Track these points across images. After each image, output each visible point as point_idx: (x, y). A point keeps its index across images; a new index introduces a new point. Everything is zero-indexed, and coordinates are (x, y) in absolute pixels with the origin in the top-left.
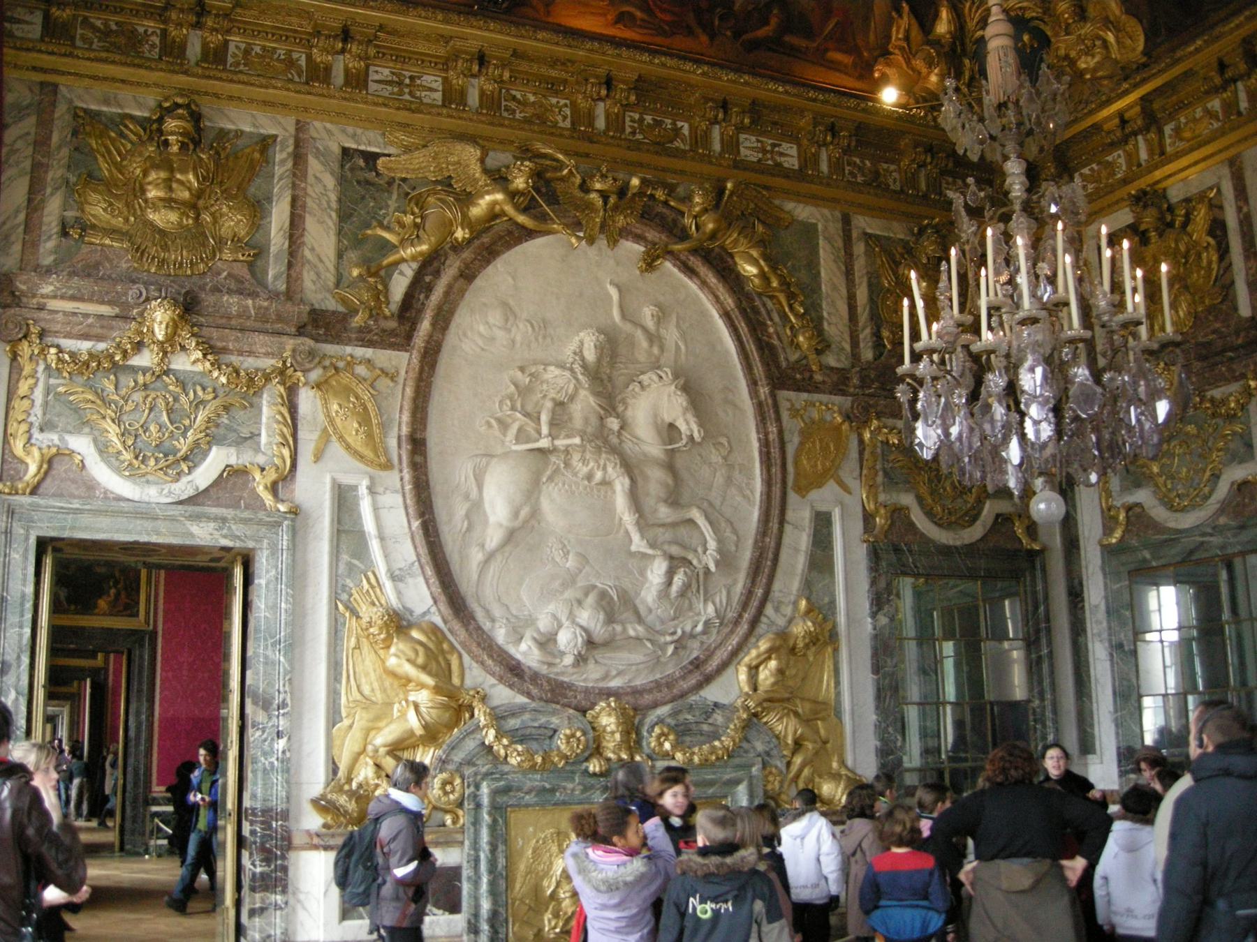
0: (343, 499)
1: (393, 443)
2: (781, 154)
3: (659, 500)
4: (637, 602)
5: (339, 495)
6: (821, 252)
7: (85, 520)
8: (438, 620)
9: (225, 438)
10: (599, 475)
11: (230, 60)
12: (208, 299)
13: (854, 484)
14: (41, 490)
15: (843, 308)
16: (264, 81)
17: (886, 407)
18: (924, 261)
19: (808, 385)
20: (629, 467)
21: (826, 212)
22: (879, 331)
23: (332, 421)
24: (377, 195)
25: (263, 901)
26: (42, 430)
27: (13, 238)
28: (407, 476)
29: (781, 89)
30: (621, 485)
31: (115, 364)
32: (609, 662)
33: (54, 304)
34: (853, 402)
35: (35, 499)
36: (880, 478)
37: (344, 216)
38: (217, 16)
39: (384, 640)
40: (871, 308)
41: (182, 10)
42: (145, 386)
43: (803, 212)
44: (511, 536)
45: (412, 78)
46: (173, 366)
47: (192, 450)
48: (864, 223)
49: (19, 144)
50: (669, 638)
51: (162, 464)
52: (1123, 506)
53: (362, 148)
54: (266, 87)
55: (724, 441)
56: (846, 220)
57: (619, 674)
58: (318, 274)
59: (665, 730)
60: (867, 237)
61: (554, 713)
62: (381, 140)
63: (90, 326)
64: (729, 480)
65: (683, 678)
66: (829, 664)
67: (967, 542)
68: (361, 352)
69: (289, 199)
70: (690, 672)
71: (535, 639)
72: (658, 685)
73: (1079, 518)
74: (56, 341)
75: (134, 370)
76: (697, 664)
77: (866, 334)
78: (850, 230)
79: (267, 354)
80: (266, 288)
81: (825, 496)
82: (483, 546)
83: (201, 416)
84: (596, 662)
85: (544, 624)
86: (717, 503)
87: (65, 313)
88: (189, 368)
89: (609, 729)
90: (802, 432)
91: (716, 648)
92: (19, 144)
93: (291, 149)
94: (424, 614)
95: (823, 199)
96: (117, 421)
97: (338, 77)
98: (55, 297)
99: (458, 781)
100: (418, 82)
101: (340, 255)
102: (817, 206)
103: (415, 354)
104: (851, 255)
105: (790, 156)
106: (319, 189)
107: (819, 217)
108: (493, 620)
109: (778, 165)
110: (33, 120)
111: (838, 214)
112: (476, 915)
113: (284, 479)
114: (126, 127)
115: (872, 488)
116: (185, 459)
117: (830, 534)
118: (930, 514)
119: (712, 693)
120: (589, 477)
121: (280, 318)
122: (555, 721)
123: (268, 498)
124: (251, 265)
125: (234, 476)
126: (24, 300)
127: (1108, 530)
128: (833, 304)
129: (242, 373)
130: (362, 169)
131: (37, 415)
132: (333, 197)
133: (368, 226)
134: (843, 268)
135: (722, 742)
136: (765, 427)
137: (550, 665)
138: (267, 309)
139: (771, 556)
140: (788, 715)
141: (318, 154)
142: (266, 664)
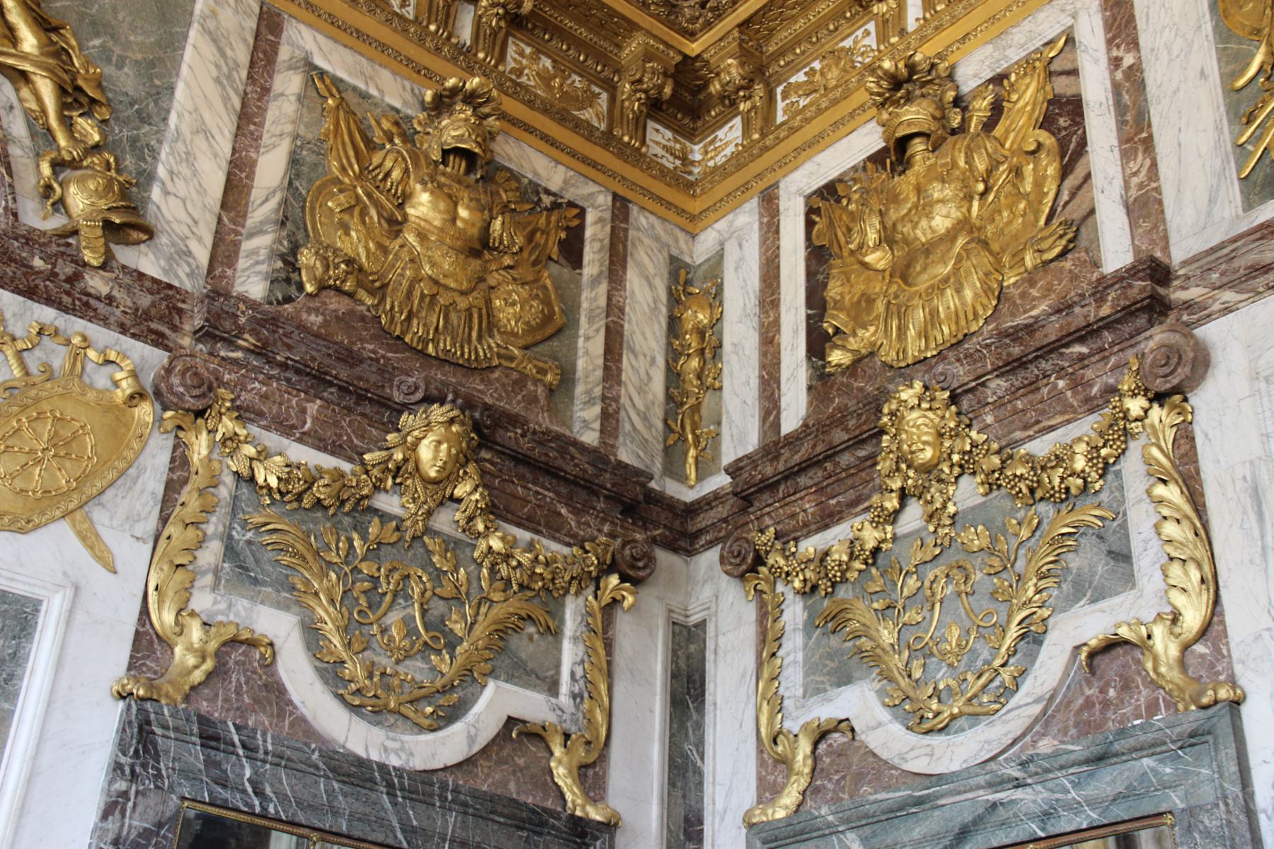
6: (189, 53)
13: (133, 555)
17: (265, 397)
18: (436, 156)
19: (66, 293)
22: (295, 249)
36: (211, 554)
40: (285, 202)
67: (418, 764)
73: (707, 769)
78: (275, 47)
104: (266, 90)
118: (332, 674)
127: (768, 790)
128: (189, 158)
134: (237, 103)
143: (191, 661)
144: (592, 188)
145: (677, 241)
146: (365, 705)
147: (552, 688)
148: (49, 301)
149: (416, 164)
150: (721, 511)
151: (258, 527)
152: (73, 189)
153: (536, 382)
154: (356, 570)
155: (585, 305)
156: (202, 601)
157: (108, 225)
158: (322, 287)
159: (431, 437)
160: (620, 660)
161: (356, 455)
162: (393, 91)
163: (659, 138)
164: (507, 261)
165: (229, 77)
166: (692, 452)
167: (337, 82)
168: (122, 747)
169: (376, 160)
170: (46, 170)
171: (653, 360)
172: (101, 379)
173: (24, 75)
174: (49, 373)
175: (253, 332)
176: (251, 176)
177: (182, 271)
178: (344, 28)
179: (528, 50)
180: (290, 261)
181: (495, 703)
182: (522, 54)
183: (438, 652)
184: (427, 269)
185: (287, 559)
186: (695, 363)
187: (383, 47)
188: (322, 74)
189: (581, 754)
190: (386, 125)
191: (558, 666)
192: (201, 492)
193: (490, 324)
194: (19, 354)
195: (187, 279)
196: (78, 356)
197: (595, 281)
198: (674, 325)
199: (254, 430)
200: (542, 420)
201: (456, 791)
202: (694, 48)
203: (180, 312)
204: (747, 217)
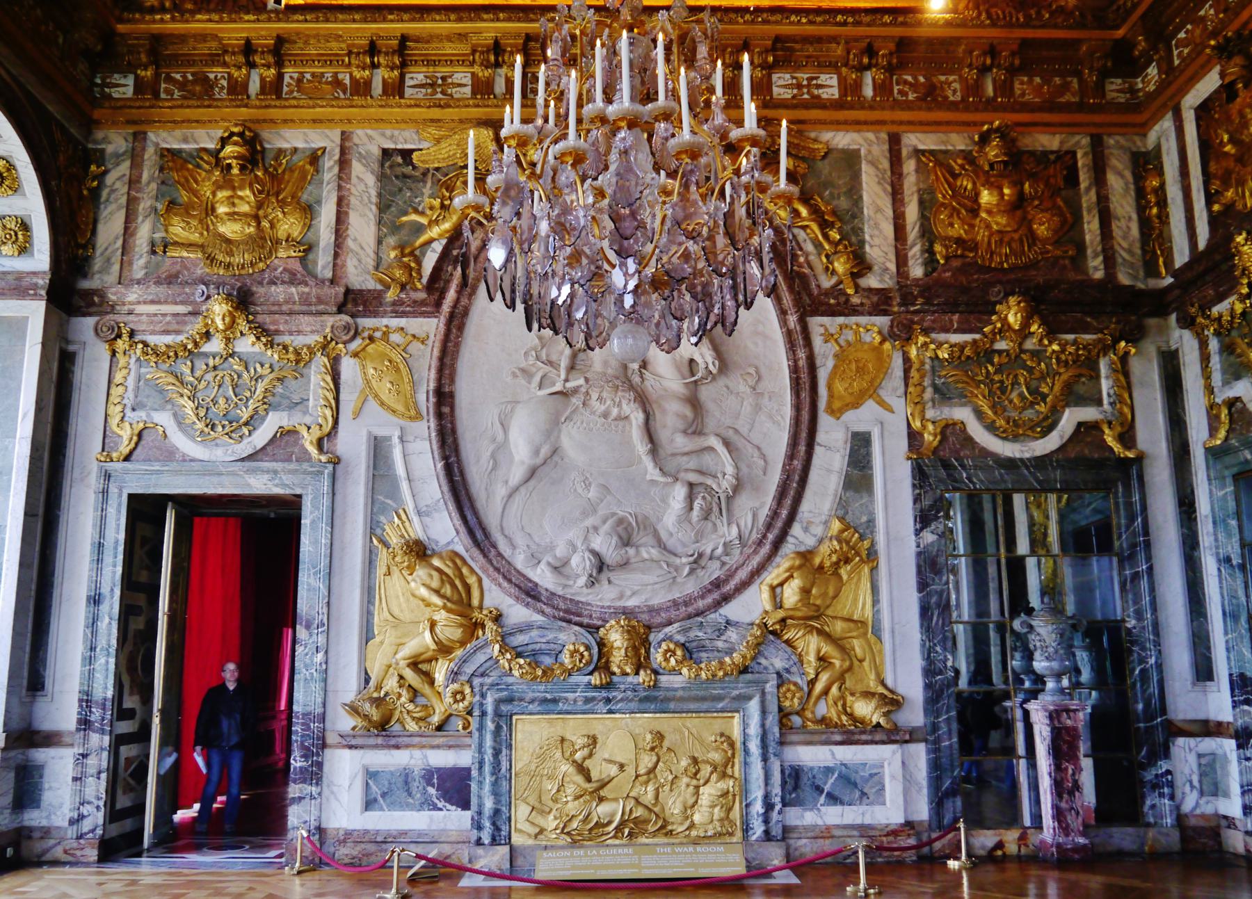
0: (378, 449)
1: (422, 397)
2: (819, 86)
3: (675, 431)
4: (659, 527)
5: (375, 446)
6: (864, 177)
7: (165, 478)
8: (460, 549)
9: (279, 405)
10: (615, 412)
11: (285, 89)
12: (260, 291)
13: (898, 404)
14: (134, 457)
15: (889, 230)
16: (311, 103)
17: (933, 321)
18: (987, 168)
19: (846, 309)
20: (643, 400)
21: (871, 136)
22: (931, 246)
23: (368, 382)
24: (413, 186)
25: (301, 790)
26: (134, 410)
27: (113, 260)
28: (433, 424)
29: (804, 20)
30: (638, 417)
31: (190, 352)
32: (623, 583)
33: (140, 309)
34: (892, 321)
35: (126, 464)
36: (929, 393)
37: (383, 207)
38: (263, 53)
39: (408, 567)
40: (922, 225)
41: (234, 53)
42: (215, 368)
43: (842, 139)
44: (532, 473)
45: (443, 78)
46: (236, 350)
47: (252, 417)
48: (913, 140)
49: (118, 185)
50: (684, 560)
51: (227, 429)
52: (1224, 401)
53: (400, 147)
54: (314, 107)
55: (752, 371)
56: (894, 142)
57: (634, 594)
58: (359, 261)
59: (672, 646)
60: (917, 153)
61: (560, 629)
62: (416, 137)
63: (168, 323)
64: (758, 408)
65: (703, 597)
66: (866, 585)
67: (1038, 453)
68: (395, 322)
69: (335, 200)
70: (709, 591)
71: (549, 564)
72: (675, 604)
74: (144, 338)
75: (206, 355)
76: (717, 584)
77: (915, 252)
78: (899, 151)
79: (313, 332)
80: (316, 277)
81: (864, 417)
82: (507, 482)
83: (261, 387)
84: (610, 582)
85: (561, 551)
86: (744, 431)
87: (148, 315)
88: (251, 349)
89: (615, 645)
90: (836, 356)
91: (737, 569)
92: (118, 185)
93: (337, 157)
94: (449, 543)
95: (866, 123)
96: (192, 398)
97: (377, 88)
98: (139, 303)
99: (467, 690)
100: (450, 80)
101: (380, 242)
102: (858, 131)
103: (443, 319)
105: (829, 85)
106: (361, 187)
107: (861, 141)
108: (514, 547)
109: (818, 97)
110: (127, 164)
111: (884, 136)
112: (480, 813)
113: (329, 435)
114: (202, 159)
115: (919, 404)
116: (246, 424)
117: (868, 455)
118: (991, 428)
119: (731, 610)
120: (605, 415)
121: (320, 301)
122: (562, 637)
123: (313, 451)
124: (303, 260)
125: (286, 435)
126: (118, 308)
127: (1213, 431)
128: (877, 225)
129: (291, 349)
130: (399, 165)
131: (129, 399)
132: (373, 193)
133: (406, 213)
134: (889, 189)
135: (732, 658)
136: (794, 352)
137: (565, 586)
138: (308, 294)
139: (797, 478)
140: (810, 632)
141: (361, 157)
142: (309, 590)
143: (931, 438)
144: (1077, 138)
145: (1134, 143)
146: (1012, 433)
147: (1099, 402)
148: (841, 315)
149: (978, 177)
150: (1177, 292)
151: (945, 376)
152: (836, 264)
153: (1063, 258)
154: (992, 380)
155: (1085, 205)
156: (930, 414)
157: (852, 274)
158: (947, 258)
159: (1012, 312)
160: (1134, 380)
161: (978, 330)
162: (958, 142)
163: (1114, 87)
164: (1036, 203)
165: (883, 178)
166: (1161, 260)
167: (932, 152)
168: (914, 477)
169: (959, 183)
170: (824, 260)
171: (1130, 218)
172: (867, 338)
173: (807, 226)
174: (849, 344)
175: (922, 297)
176: (904, 220)
177: (887, 278)
178: (928, 124)
179: (1025, 79)
180: (930, 251)
181: (1070, 419)
182: (1022, 83)
183: (1038, 404)
184: (995, 227)
185: (960, 385)
186: (1155, 211)
187: (948, 123)
188: (923, 152)
189: (1119, 429)
190: (960, 161)
191: (1100, 392)
192: (918, 370)
193: (1032, 236)
194: (836, 340)
195: (888, 282)
196: (856, 333)
197: (1088, 190)
198: (1140, 193)
199: (933, 335)
200: (1072, 276)
201: (1057, 461)
202: (1120, 33)
203: (890, 298)
204: (1167, 123)
